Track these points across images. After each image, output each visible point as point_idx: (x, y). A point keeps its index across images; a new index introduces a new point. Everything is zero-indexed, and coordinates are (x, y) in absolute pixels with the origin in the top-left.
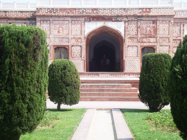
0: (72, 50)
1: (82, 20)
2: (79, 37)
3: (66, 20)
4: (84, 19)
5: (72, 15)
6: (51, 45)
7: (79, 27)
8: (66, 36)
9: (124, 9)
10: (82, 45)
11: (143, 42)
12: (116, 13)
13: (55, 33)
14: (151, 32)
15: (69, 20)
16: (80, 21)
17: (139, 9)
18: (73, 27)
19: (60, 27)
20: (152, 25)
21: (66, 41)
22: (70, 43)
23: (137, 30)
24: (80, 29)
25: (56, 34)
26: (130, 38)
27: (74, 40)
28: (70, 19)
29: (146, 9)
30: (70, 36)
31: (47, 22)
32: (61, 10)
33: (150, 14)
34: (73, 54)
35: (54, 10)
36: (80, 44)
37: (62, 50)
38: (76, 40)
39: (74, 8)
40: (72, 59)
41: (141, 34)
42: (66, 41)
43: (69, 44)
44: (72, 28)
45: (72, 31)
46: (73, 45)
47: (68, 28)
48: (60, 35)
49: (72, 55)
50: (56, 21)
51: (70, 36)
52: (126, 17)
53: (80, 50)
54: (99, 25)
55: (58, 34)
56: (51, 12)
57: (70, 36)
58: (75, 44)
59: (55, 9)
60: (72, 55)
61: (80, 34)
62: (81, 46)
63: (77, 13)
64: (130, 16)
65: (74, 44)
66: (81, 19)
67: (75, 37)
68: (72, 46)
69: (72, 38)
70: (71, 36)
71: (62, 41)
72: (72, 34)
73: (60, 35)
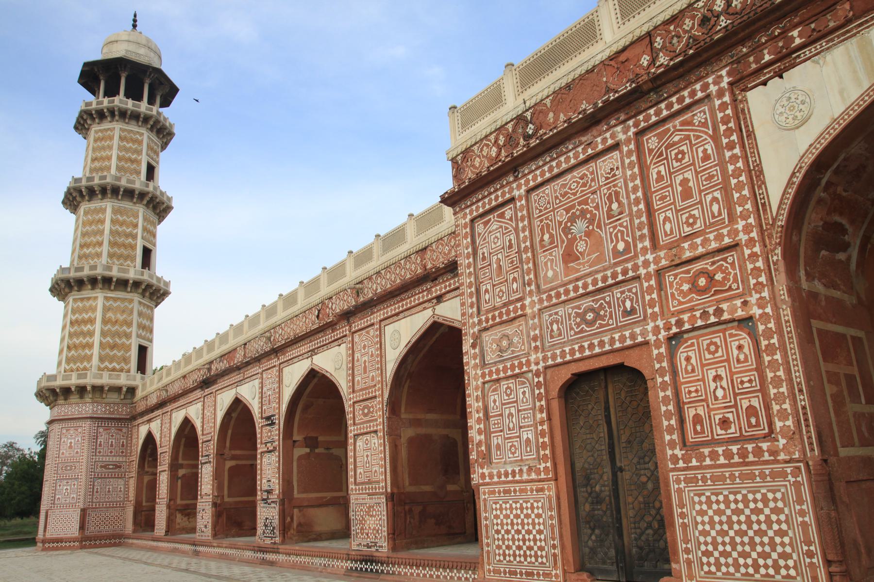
0: (682, 377)
1: (713, 89)
2: (714, 245)
3: (600, 147)
4: (729, 74)
6: (534, 367)
7: (706, 157)
8: (619, 269)
10: (756, 311)
13: (550, 274)
15: (622, 137)
16: (700, 101)
18: (660, 178)
19: (572, 220)
21: (626, 313)
22: (654, 317)
24: (716, 171)
25: (556, 274)
27: (677, 283)
28: (626, 131)
31: (502, 216)
34: (697, 419)
35: (527, 123)
36: (733, 309)
37: (615, 392)
38: (702, 282)
39: (637, 33)
40: (694, 463)
42: (626, 313)
43: (644, 333)
44: (653, 183)
45: (650, 212)
46: (674, 330)
47: (625, 201)
48: (577, 279)
49: (682, 421)
50: (547, 189)
51: (646, 264)
53: (752, 363)
55: (568, 271)
57: (646, 264)
58: (693, 319)
59: (528, 115)
60: (689, 425)
61: (725, 215)
62: (746, 322)
63: (663, 59)
65: (685, 317)
66: (705, 87)
67: (688, 255)
68: (675, 340)
69: (659, 273)
70: (650, 257)
71: (598, 317)
72: (663, 240)
73: (577, 279)
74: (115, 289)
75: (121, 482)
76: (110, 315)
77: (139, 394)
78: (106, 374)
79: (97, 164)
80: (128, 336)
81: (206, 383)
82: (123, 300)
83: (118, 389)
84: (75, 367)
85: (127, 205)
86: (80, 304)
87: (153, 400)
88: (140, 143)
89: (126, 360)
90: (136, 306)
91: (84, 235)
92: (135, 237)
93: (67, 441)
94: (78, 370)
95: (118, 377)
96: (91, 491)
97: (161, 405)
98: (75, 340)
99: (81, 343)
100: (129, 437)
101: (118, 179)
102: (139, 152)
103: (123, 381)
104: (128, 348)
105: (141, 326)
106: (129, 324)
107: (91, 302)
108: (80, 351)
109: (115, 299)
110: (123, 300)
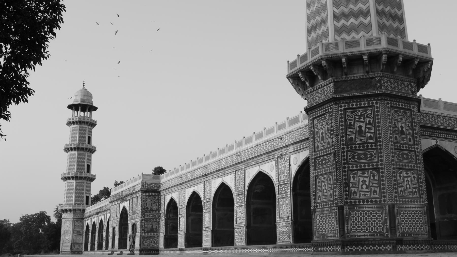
74: (79, 179)
75: (81, 237)
76: (78, 187)
77: (86, 212)
78: (76, 205)
79: (73, 139)
80: (83, 194)
81: (97, 213)
82: (81, 183)
83: (80, 210)
85: (82, 152)
86: (69, 184)
87: (88, 215)
88: (85, 130)
89: (82, 201)
90: (85, 184)
91: (70, 162)
92: (84, 162)
93: (67, 224)
95: (80, 206)
96: (73, 238)
97: (90, 216)
100: (83, 224)
102: (85, 134)
103: (81, 207)
104: (83, 197)
105: (87, 190)
106: (83, 190)
109: (79, 182)
110: (81, 183)
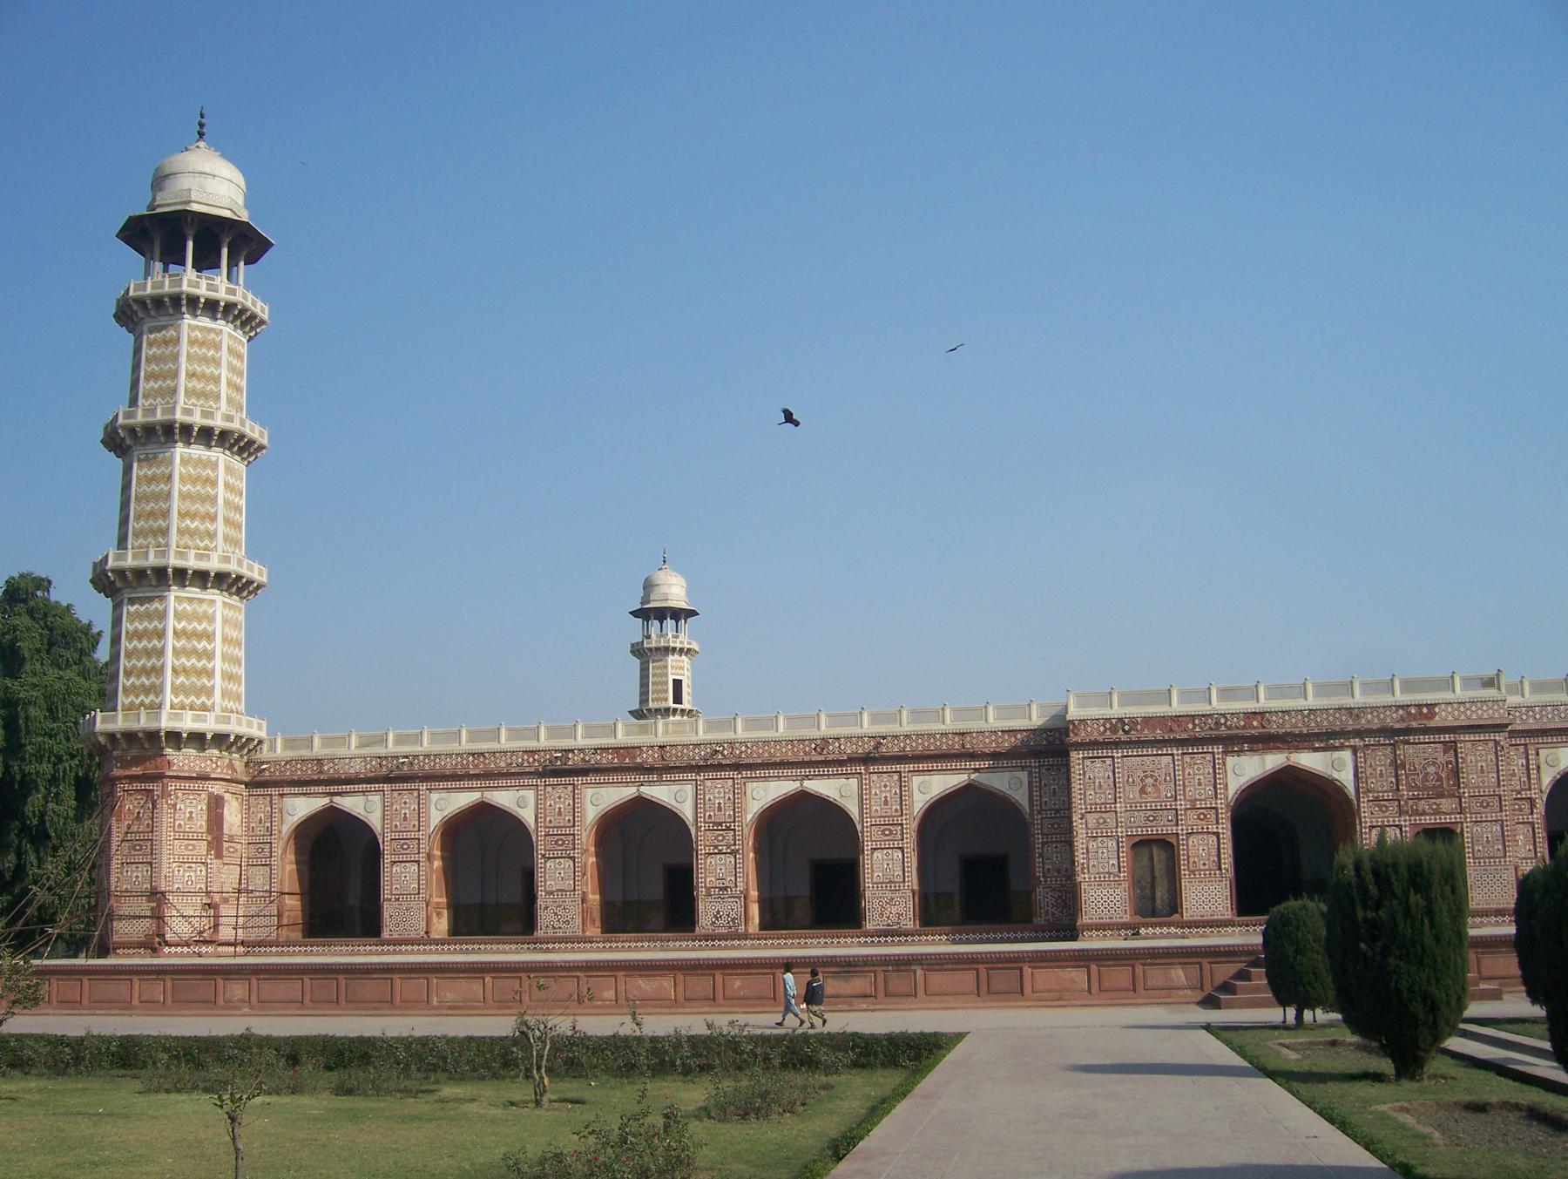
5: (1185, 736)
9: (1350, 710)
11: (1416, 813)
12: (1326, 724)
14: (1440, 779)
17: (1399, 707)
20: (1441, 758)
23: (1397, 776)
26: (1377, 799)
27: (1192, 814)
29: (1419, 706)
30: (1181, 804)
32: (1147, 720)
33: (1432, 724)
41: (1410, 788)
52: (1359, 734)
54: (1273, 761)
56: (1114, 730)
62: (1217, 834)
64: (1370, 732)
77: (265, 753)
84: (187, 702)
94: (192, 708)
98: (184, 660)
99: (193, 666)
101: (229, 418)
107: (205, 606)
108: (194, 679)
